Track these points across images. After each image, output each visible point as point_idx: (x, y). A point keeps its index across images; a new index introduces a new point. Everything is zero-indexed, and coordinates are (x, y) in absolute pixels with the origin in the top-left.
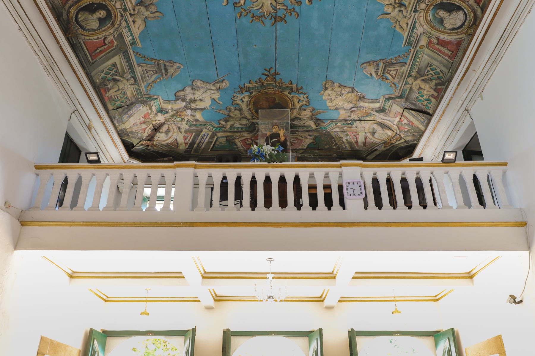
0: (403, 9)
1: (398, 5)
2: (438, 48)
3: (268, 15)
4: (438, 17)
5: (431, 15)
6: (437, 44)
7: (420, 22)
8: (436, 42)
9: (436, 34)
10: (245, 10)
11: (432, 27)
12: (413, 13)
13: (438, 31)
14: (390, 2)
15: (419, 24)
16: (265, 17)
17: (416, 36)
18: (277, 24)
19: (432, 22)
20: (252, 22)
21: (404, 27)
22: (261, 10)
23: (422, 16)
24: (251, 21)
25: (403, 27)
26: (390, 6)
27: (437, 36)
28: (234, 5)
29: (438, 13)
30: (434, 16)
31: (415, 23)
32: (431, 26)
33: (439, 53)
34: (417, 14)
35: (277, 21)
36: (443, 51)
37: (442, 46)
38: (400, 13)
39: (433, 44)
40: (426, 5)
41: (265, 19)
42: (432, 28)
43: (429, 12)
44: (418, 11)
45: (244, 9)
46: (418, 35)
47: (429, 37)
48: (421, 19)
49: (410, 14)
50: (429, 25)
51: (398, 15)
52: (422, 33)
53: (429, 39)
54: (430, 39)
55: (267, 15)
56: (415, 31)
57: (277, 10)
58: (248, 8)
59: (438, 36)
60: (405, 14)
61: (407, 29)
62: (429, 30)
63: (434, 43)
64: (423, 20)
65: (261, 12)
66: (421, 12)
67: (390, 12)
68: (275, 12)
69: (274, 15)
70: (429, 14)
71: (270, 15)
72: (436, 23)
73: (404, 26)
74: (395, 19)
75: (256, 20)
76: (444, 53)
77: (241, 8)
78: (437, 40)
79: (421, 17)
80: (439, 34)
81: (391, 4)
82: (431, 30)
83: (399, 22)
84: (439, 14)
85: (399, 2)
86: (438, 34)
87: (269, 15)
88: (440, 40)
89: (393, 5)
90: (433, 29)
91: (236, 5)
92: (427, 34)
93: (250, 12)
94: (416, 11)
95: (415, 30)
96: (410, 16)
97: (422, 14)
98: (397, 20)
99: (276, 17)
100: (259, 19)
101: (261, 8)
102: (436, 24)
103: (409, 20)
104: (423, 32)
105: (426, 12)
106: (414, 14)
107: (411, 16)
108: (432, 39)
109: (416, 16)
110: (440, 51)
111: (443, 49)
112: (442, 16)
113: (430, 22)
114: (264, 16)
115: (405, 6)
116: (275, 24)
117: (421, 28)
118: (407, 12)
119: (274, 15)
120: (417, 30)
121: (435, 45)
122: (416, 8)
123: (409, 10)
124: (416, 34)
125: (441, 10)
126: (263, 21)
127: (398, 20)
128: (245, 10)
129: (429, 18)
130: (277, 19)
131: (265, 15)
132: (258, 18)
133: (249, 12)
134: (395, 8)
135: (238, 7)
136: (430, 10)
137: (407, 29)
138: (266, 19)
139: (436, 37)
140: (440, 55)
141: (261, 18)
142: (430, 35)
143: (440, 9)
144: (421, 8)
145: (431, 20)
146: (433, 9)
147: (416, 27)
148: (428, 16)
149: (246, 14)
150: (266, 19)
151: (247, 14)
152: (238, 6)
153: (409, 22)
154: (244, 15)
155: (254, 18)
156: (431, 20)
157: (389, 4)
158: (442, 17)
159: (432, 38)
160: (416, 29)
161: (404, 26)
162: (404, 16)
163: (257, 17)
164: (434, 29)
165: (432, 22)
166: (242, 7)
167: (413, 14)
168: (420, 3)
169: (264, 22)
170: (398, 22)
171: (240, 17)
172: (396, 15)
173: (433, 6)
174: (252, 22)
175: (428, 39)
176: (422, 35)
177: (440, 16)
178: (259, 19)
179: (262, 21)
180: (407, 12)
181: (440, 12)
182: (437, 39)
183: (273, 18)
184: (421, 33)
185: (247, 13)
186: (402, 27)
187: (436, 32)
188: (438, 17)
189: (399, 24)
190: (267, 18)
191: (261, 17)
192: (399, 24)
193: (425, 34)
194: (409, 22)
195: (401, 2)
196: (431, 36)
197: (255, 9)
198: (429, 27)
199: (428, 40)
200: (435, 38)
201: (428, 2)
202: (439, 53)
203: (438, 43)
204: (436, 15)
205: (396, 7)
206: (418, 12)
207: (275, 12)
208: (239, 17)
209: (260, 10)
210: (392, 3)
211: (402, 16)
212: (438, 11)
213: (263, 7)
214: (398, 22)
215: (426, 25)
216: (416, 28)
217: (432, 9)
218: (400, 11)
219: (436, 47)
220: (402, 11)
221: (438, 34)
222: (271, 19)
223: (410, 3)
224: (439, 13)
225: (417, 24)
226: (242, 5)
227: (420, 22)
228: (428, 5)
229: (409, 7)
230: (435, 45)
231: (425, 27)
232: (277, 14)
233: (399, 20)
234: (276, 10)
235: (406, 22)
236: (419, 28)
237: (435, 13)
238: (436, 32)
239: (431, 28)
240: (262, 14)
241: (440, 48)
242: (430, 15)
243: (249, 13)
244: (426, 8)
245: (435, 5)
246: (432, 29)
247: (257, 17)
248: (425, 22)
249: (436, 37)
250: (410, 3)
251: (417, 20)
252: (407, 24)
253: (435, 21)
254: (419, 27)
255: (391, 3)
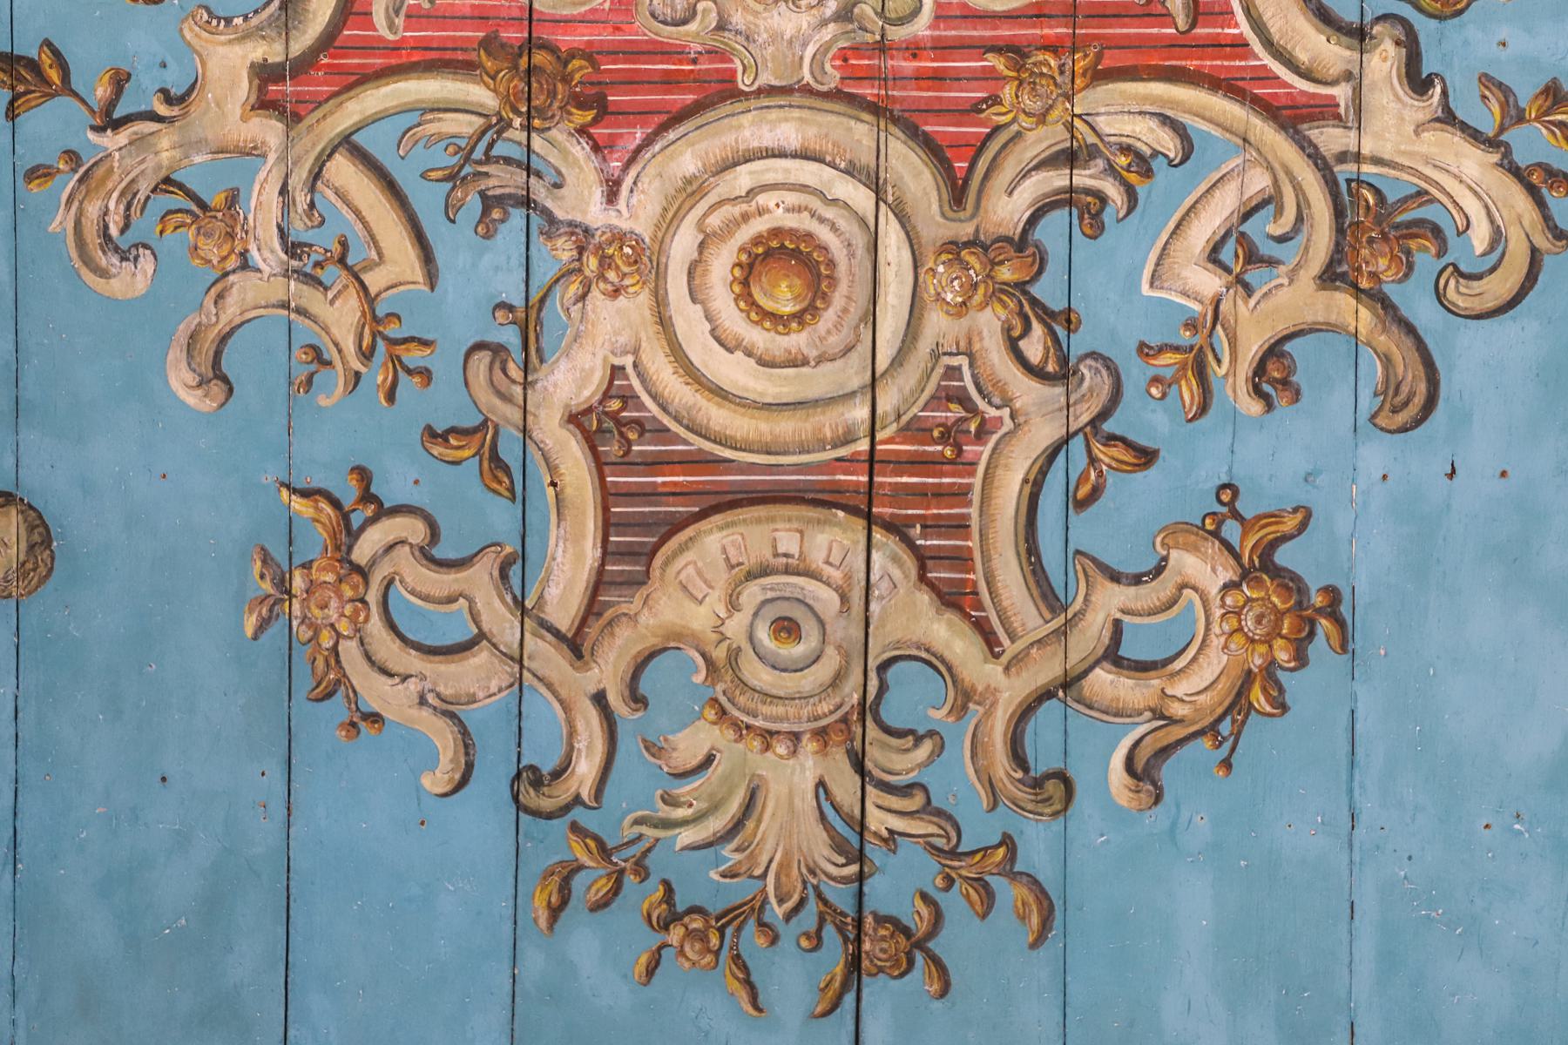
3: (796, 898)
10: (604, 852)
16: (762, 924)
18: (865, 992)
20: (650, 972)
22: (737, 850)
24: (644, 959)
28: (519, 806)
35: (865, 963)
41: (761, 942)
45: (596, 839)
55: (781, 901)
57: (868, 848)
58: (629, 833)
65: (730, 874)
68: (854, 868)
69: (841, 897)
71: (812, 906)
75: (687, 948)
77: (575, 828)
87: (802, 902)
91: (530, 797)
93: (641, 870)
99: (859, 923)
100: (714, 941)
101: (737, 826)
114: (755, 908)
116: (849, 999)
119: (841, 897)
126: (745, 968)
128: (604, 852)
130: (867, 946)
131: (765, 901)
132: (700, 935)
133: (636, 873)
135: (550, 816)
138: (774, 940)
141: (729, 931)
149: (604, 886)
150: (774, 940)
151: (616, 890)
152: (546, 804)
154: (593, 896)
155: (675, 935)
163: (697, 923)
166: (578, 814)
169: (754, 978)
171: (555, 912)
174: (650, 972)
178: (714, 941)
179: (737, 959)
183: (829, 931)
185: (622, 872)
190: (781, 927)
191: (731, 917)
197: (687, 836)
207: (853, 869)
208: (543, 917)
209: (729, 854)
213: (750, 824)
222: (817, 939)
226: (585, 794)
232: (866, 889)
234: (861, 857)
240: (741, 890)
243: (630, 880)
247: (697, 923)
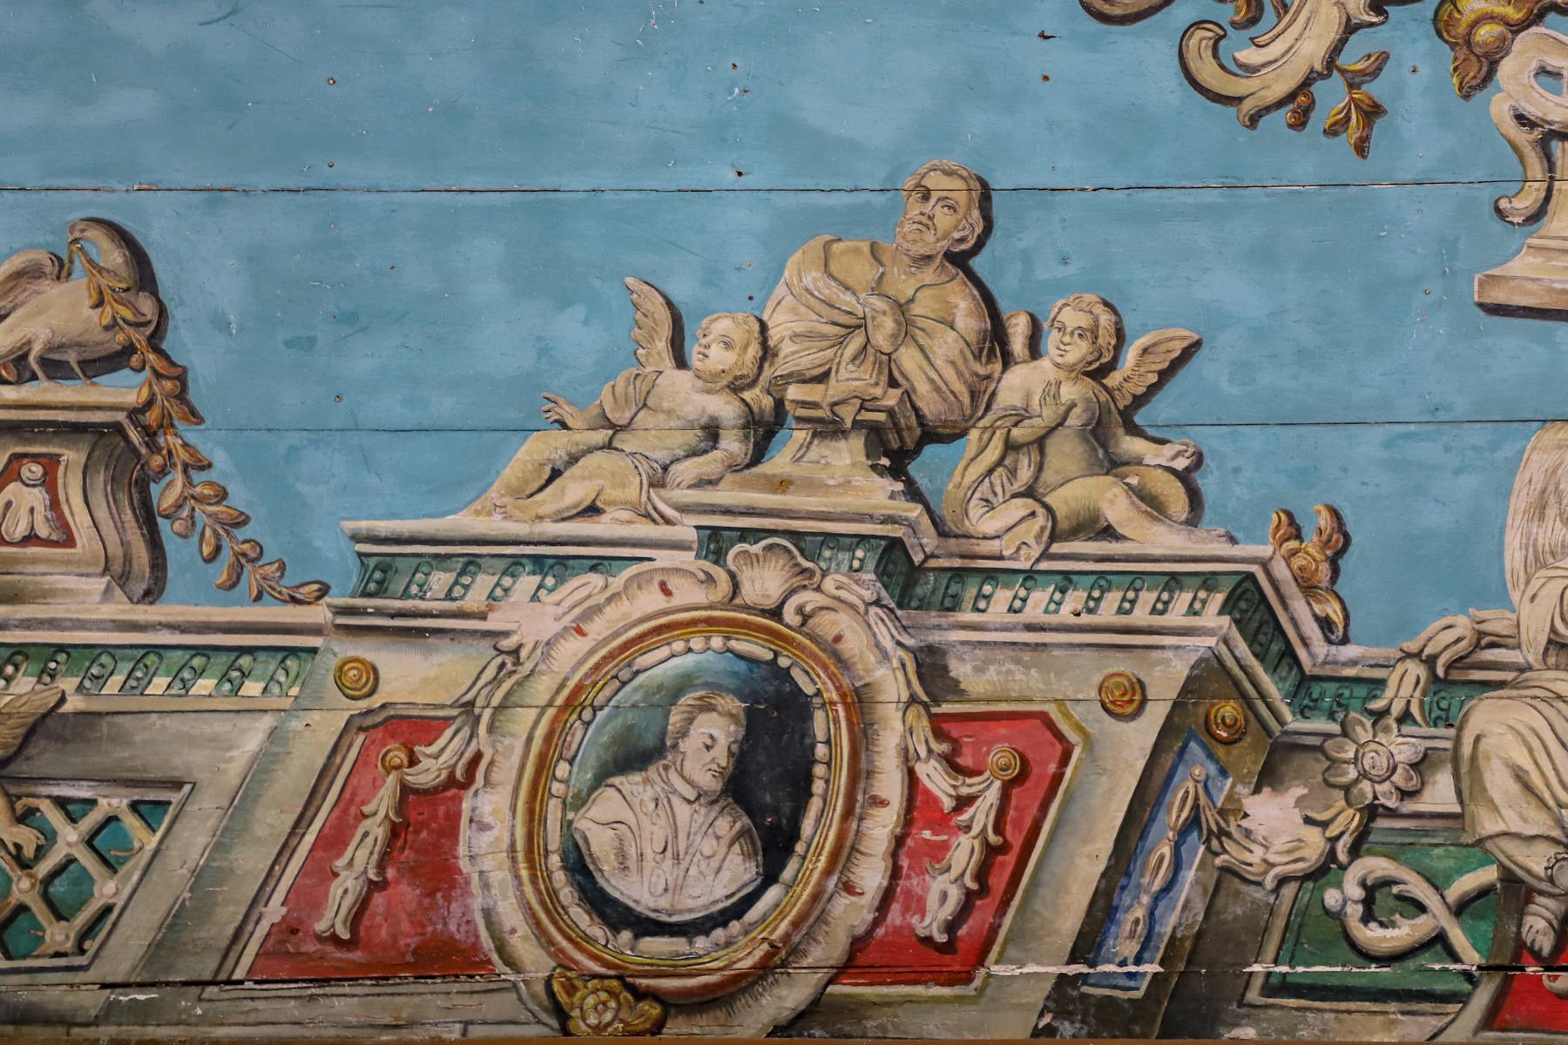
0: (733, 445)
1: (768, 402)
2: (366, 809)
4: (672, 719)
5: (690, 659)
6: (405, 789)
7: (609, 600)
8: (428, 773)
9: (511, 749)
11: (574, 703)
12: (697, 527)
13: (543, 760)
14: (787, 348)
15: (601, 599)
17: (475, 598)
19: (624, 684)
21: (563, 489)
23: (677, 601)
25: (557, 482)
26: (754, 350)
27: (492, 763)
29: (711, 708)
30: (683, 684)
31: (596, 564)
32: (579, 689)
33: (310, 838)
34: (686, 559)
36: (340, 863)
37: (395, 832)
38: (693, 438)
39: (399, 756)
40: (770, 603)
42: (569, 704)
43: (717, 642)
44: (718, 557)
46: (483, 616)
47: (471, 704)
48: (651, 601)
49: (684, 509)
50: (587, 676)
51: (673, 424)
52: (506, 644)
53: (455, 712)
54: (448, 720)
56: (527, 582)
59: (486, 778)
60: (688, 470)
61: (540, 518)
62: (542, 689)
63: (413, 761)
64: (636, 615)
66: (710, 579)
67: (694, 359)
70: (697, 643)
72: (618, 722)
73: (574, 490)
74: (628, 415)
76: (320, 872)
78: (452, 774)
79: (661, 596)
80: (514, 774)
81: (767, 353)
82: (543, 699)
83: (609, 446)
84: (702, 718)
85: (788, 406)
86: (506, 772)
88: (458, 800)
89: (761, 368)
90: (551, 712)
92: (496, 681)
94: (715, 543)
95: (537, 579)
96: (670, 512)
97: (688, 594)
98: (617, 429)
102: (609, 718)
103: (625, 515)
104: (515, 652)
105: (709, 621)
106: (692, 535)
107: (668, 522)
108: (448, 733)
109: (664, 558)
110: (333, 841)
111: (361, 856)
112: (684, 746)
113: (624, 675)
115: (757, 458)
117: (558, 619)
118: (703, 483)
120: (535, 598)
121: (392, 779)
122: (742, 539)
123: (724, 495)
124: (491, 596)
125: (737, 723)
127: (620, 436)
129: (664, 652)
134: (736, 387)
136: (733, 644)
137: (540, 518)
139: (478, 756)
140: (286, 850)
142: (487, 713)
143: (750, 713)
144: (745, 576)
145: (641, 678)
146: (742, 666)
147: (560, 580)
148: (678, 646)
153: (612, 513)
156: (637, 673)
157: (771, 343)
158: (675, 746)
159: (466, 731)
160: (540, 586)
161: (574, 490)
162: (665, 468)
164: (555, 720)
165: (628, 688)
167: (686, 530)
168: (794, 557)
170: (601, 436)
172: (669, 412)
173: (770, 656)
175: (451, 706)
176: (486, 644)
177: (684, 734)
180: (703, 483)
181: (722, 721)
182: (459, 774)
184: (506, 634)
186: (556, 474)
187: (530, 739)
188: (675, 718)
189: (591, 450)
192: (591, 450)
193: (503, 665)
194: (604, 518)
195: (790, 422)
196: (478, 719)
198: (571, 684)
199: (443, 706)
200: (469, 754)
201: (800, 610)
202: (310, 838)
203: (416, 792)
204: (687, 700)
205: (747, 395)
206: (707, 565)
210: (779, 360)
211: (662, 456)
212: (734, 705)
214: (601, 436)
215: (591, 652)
216: (550, 581)
217: (740, 656)
218: (712, 432)
219: (375, 786)
220: (714, 448)
221: (506, 772)
223: (783, 485)
224: (714, 714)
225: (596, 579)
227: (609, 600)
228: (776, 613)
229: (743, 486)
230: (392, 779)
231: (573, 648)
233: (627, 442)
235: (611, 493)
236: (558, 604)
237: (706, 685)
238: (530, 739)
239: (566, 692)
241: (366, 824)
242: (690, 650)
244: (747, 608)
245: (783, 662)
246: (559, 701)
248: (616, 635)
249: (478, 756)
250: (783, 485)
251: (635, 569)
252: (592, 510)
253: (634, 706)
254: (560, 610)
255: (776, 355)
